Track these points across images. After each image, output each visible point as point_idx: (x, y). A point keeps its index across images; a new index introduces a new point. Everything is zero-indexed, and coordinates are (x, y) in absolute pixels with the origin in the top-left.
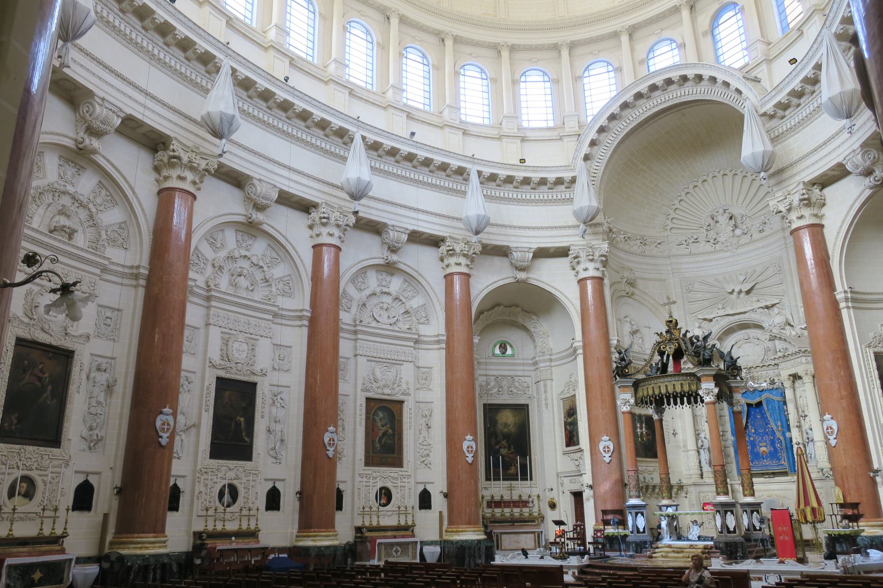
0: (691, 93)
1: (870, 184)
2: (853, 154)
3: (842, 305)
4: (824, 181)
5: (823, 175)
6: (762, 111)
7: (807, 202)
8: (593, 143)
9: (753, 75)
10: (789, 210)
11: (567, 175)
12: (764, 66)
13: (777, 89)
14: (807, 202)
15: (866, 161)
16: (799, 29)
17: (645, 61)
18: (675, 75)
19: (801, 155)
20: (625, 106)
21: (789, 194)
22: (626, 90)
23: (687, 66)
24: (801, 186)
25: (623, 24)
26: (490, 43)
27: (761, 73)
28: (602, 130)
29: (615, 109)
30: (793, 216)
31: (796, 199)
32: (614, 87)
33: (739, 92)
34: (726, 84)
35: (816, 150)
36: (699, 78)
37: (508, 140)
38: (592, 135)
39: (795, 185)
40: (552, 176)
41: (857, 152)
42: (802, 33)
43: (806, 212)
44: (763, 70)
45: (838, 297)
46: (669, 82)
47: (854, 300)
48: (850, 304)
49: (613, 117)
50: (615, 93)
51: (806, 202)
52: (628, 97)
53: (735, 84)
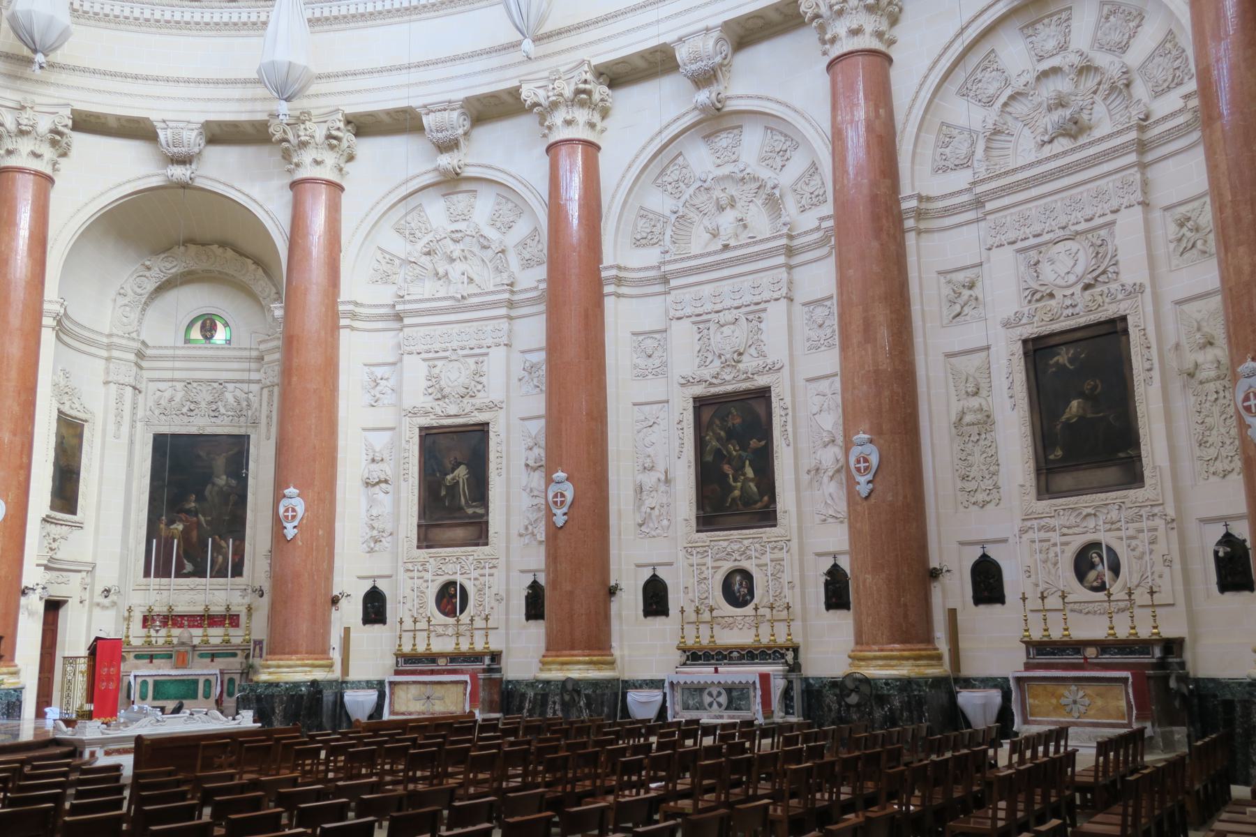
1: (183, 178)
2: (185, 124)
3: (47, 321)
4: (86, 123)
5: (97, 116)
7: (56, 139)
10: (22, 133)
14: (56, 139)
15: (195, 145)
19: (72, 62)
21: (32, 108)
24: (68, 112)
30: (25, 146)
31: (44, 125)
35: (114, 75)
39: (56, 101)
41: (194, 126)
43: (48, 152)
45: (46, 306)
47: (59, 323)
48: (55, 323)
51: (58, 138)
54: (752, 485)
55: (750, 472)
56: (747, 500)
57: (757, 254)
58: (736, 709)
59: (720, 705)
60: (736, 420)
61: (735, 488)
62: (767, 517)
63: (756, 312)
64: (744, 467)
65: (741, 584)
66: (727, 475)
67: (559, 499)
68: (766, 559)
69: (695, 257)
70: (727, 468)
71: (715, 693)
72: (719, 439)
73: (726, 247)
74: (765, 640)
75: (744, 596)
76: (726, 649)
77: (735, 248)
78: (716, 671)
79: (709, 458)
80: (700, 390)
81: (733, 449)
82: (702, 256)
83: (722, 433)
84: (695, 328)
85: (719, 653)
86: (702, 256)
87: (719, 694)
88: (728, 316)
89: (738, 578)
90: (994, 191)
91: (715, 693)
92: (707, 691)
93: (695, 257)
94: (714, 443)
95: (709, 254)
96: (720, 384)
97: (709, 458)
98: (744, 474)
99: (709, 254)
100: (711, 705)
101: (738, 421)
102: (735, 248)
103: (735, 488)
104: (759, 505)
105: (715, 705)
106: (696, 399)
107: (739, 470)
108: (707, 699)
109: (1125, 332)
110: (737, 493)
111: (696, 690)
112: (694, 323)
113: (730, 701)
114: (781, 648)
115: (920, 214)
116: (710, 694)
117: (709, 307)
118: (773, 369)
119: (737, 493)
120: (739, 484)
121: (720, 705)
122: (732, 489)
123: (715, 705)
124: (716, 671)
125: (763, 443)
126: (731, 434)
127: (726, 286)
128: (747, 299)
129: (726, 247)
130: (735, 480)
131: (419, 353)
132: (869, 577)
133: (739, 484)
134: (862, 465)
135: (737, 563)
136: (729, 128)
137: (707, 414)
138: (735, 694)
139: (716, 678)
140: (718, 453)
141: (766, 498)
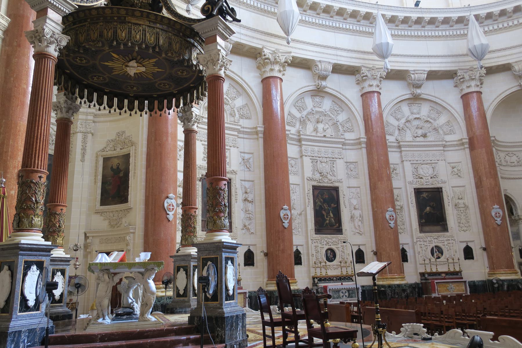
54: (333, 220)
55: (332, 215)
56: (331, 225)
57: (334, 142)
58: (351, 297)
59: (346, 296)
60: (326, 196)
61: (327, 220)
62: (339, 230)
63: (333, 160)
64: (330, 213)
65: (330, 254)
66: (324, 215)
67: (286, 217)
68: (339, 246)
69: (307, 135)
70: (324, 212)
71: (344, 292)
72: (321, 202)
73: (325, 136)
74: (344, 273)
75: (332, 258)
76: (332, 277)
77: (328, 137)
78: (342, 284)
79: (318, 208)
80: (315, 184)
81: (326, 206)
82: (309, 136)
83: (322, 200)
84: (311, 161)
85: (330, 278)
86: (309, 136)
87: (346, 292)
88: (325, 160)
89: (329, 252)
90: (406, 145)
91: (344, 292)
92: (341, 292)
93: (307, 135)
94: (319, 203)
95: (312, 136)
96: (322, 183)
97: (318, 208)
98: (330, 215)
99: (312, 136)
100: (343, 296)
101: (327, 197)
102: (328, 137)
103: (327, 220)
104: (335, 227)
105: (344, 296)
106: (313, 186)
107: (328, 213)
108: (341, 294)
109: (442, 191)
110: (328, 222)
111: (337, 291)
112: (311, 159)
113: (349, 295)
114: (350, 276)
115: (360, 143)
116: (342, 293)
117: (316, 155)
118: (340, 181)
119: (328, 222)
120: (328, 219)
121: (346, 296)
122: (327, 220)
123: (344, 296)
124: (342, 284)
125: (336, 205)
126: (325, 201)
127: (330, 150)
128: (330, 156)
129: (325, 136)
130: (327, 217)
131: (201, 141)
132: (394, 253)
133: (328, 219)
134: (392, 218)
135: (330, 246)
136: (321, 96)
137: (317, 192)
138: (350, 292)
139: (341, 287)
140: (320, 207)
141: (337, 225)
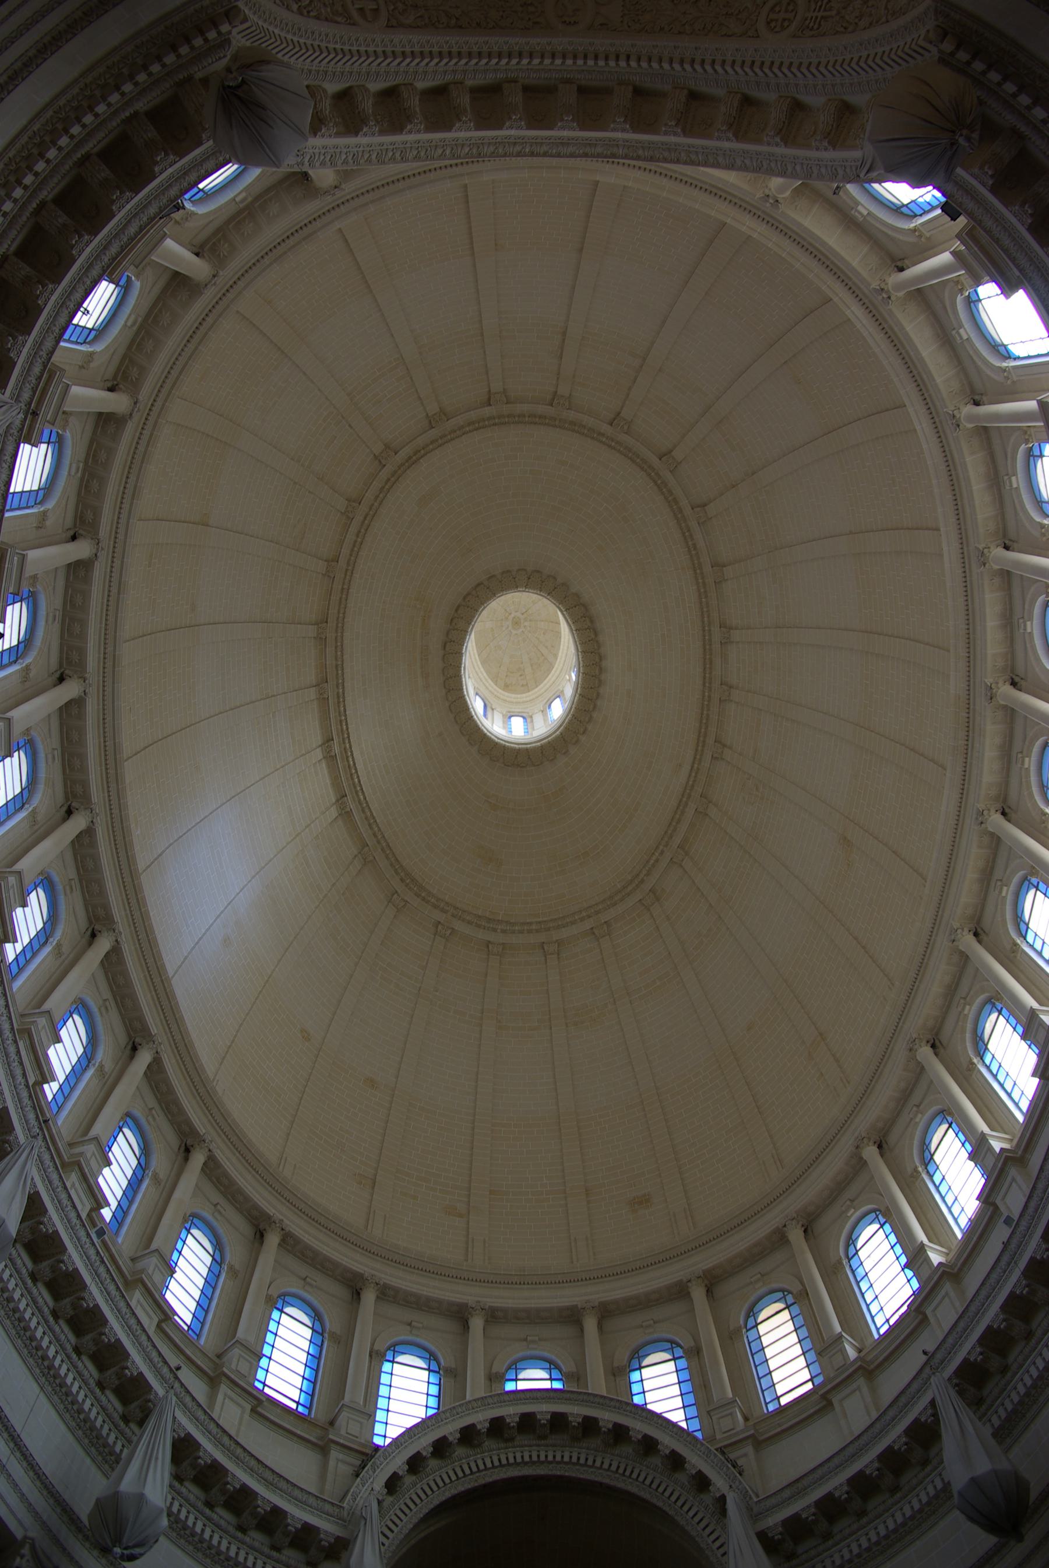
0: (590, 1462)
6: (762, 1525)
8: (392, 1484)
9: (732, 1456)
11: (327, 1526)
12: (749, 1449)
13: (797, 1486)
16: (824, 1396)
17: (502, 1379)
18: (576, 1411)
20: (468, 1435)
22: (482, 1402)
23: (602, 1401)
25: (479, 1299)
26: (256, 1207)
27: (746, 1456)
28: (415, 1464)
29: (451, 1429)
32: (433, 1402)
33: (702, 1483)
34: (676, 1461)
36: (620, 1433)
37: (229, 1392)
38: (398, 1463)
40: (298, 1514)
42: (830, 1404)
44: (745, 1455)
46: (558, 1422)
49: (441, 1448)
50: (431, 1412)
52: (481, 1418)
53: (696, 1461)
